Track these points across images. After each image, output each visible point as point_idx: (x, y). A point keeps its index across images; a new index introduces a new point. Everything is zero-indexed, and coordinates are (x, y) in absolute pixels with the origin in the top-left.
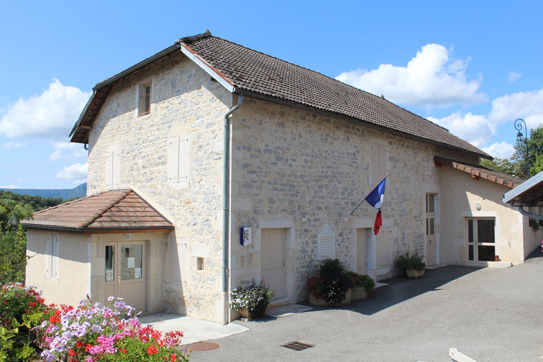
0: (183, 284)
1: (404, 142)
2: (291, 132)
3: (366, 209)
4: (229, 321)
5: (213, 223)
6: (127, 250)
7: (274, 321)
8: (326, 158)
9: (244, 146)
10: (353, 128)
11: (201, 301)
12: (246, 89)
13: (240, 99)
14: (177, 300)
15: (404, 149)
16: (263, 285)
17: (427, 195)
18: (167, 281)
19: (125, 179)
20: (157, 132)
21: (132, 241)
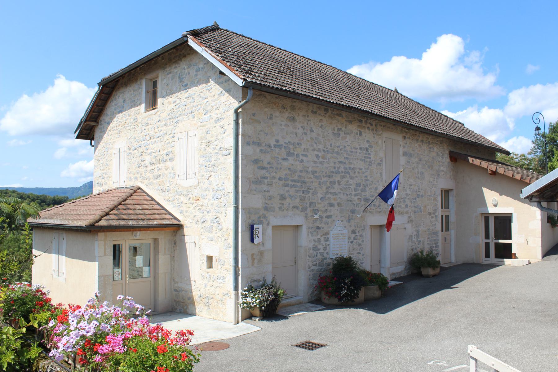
0: (193, 283)
1: (419, 136)
2: (302, 127)
3: (379, 206)
4: (240, 320)
5: (222, 220)
6: (135, 248)
7: (286, 320)
8: (338, 153)
9: (253, 142)
10: (366, 122)
11: (211, 301)
12: (256, 82)
13: (250, 93)
14: (186, 299)
15: (419, 143)
16: (274, 284)
17: (442, 191)
18: (176, 280)
19: (132, 176)
20: (165, 128)
21: (140, 239)
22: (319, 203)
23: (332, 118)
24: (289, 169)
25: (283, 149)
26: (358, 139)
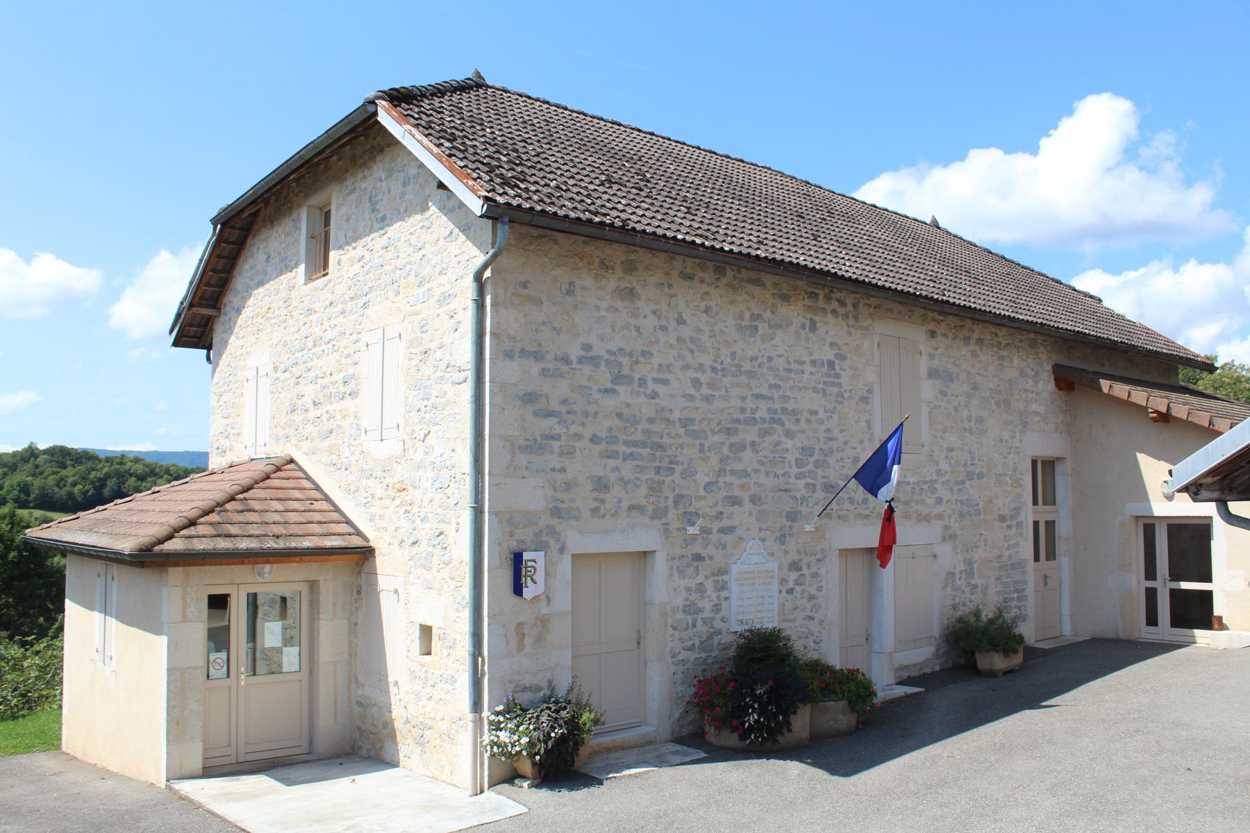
0: (393, 689)
2: (654, 312)
4: (486, 785)
5: (451, 540)
6: (284, 600)
7: (595, 790)
8: (751, 375)
9: (523, 351)
10: (828, 299)
11: (427, 733)
12: (519, 206)
15: (972, 347)
16: (573, 697)
17: (1034, 463)
18: (361, 680)
20: (341, 319)
21: (272, 581)
22: (701, 498)
23: (735, 289)
24: (620, 415)
25: (603, 367)
26: (807, 339)
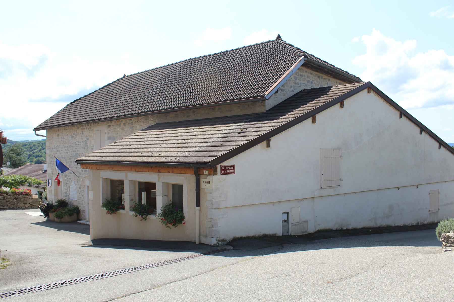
10: (85, 125)
